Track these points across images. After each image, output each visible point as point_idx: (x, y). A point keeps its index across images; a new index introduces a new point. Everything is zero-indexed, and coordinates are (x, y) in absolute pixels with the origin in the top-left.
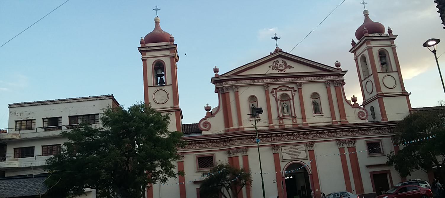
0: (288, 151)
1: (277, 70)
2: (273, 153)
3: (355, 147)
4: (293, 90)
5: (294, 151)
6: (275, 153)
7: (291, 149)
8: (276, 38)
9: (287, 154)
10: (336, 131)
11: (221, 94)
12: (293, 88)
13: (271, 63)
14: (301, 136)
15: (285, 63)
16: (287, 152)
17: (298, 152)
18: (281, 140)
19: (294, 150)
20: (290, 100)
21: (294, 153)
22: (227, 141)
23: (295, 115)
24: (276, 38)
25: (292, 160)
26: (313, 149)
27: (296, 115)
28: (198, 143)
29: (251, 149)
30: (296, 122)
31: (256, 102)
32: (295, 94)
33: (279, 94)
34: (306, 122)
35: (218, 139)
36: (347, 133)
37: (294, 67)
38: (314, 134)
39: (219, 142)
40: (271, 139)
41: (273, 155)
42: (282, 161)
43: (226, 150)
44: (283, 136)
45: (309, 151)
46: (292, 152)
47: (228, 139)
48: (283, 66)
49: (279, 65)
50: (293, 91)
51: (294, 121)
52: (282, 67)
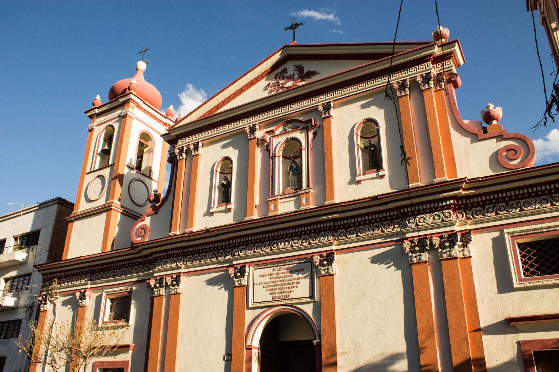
0: (267, 279)
3: (470, 257)
5: (284, 281)
7: (275, 274)
10: (402, 211)
15: (300, 69)
17: (291, 282)
23: (308, 186)
25: (276, 304)
28: (112, 270)
33: (278, 143)
36: (439, 216)
38: (341, 229)
42: (252, 306)
46: (277, 281)
48: (296, 76)
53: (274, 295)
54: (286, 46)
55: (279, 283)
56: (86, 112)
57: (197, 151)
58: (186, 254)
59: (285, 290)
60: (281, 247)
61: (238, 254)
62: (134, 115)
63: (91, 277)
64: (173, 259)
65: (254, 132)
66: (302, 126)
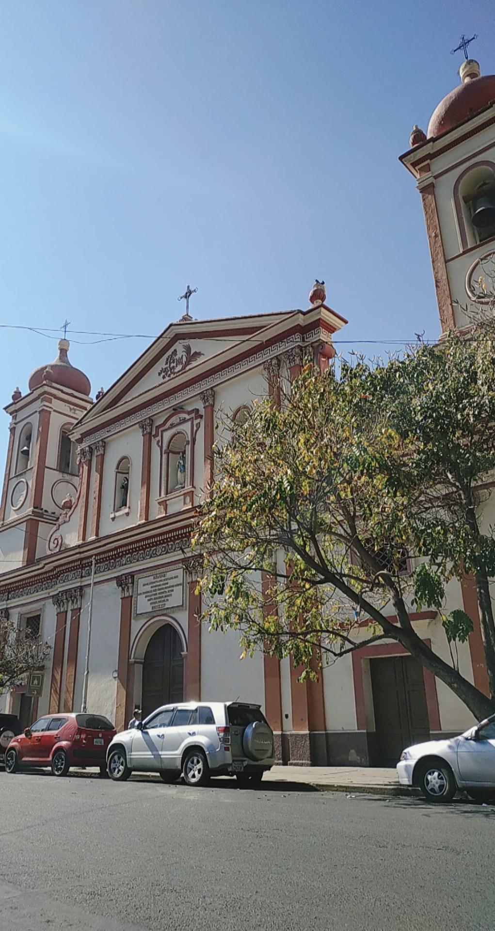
1: (172, 376)
4: (193, 415)
9: (146, 597)
13: (162, 364)
14: (177, 542)
15: (188, 349)
17: (166, 590)
18: (138, 561)
19: (160, 585)
21: (159, 594)
28: (25, 587)
29: (89, 591)
32: (198, 425)
33: (167, 435)
37: (204, 353)
39: (49, 578)
43: (53, 596)
44: (144, 549)
46: (155, 590)
48: (184, 359)
53: (154, 605)
54: (171, 325)
56: (5, 409)
59: (163, 599)
60: (158, 554)
62: (50, 408)
63: (8, 596)
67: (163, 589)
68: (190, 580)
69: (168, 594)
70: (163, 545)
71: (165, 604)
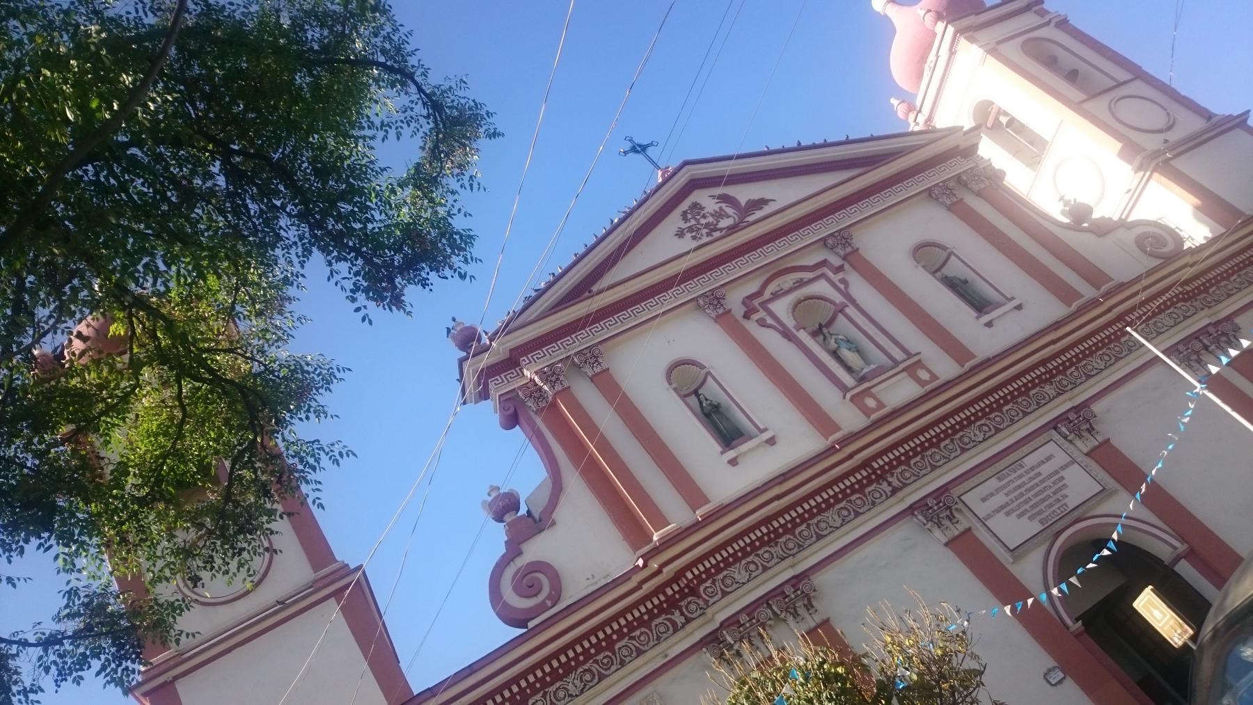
0: (1000, 499)
1: (717, 234)
2: (947, 545)
6: (955, 538)
7: (1008, 484)
8: (639, 149)
9: (1008, 514)
11: (536, 414)
12: (824, 263)
13: (674, 221)
16: (1002, 507)
17: (1049, 483)
19: (1024, 484)
20: (841, 311)
21: (1036, 495)
22: (682, 599)
24: (639, 149)
26: (1100, 439)
27: (913, 353)
28: (535, 692)
30: (934, 377)
31: (710, 379)
33: (781, 307)
34: (974, 357)
35: (629, 609)
39: (641, 622)
40: (885, 484)
41: (949, 553)
44: (932, 445)
45: (1087, 454)
46: (1022, 495)
47: (683, 582)
48: (730, 211)
49: (712, 215)
50: (831, 274)
51: (924, 375)
52: (728, 217)
54: (686, 163)
55: (1030, 494)
57: (599, 364)
58: (772, 536)
59: (1051, 500)
60: (981, 439)
61: (900, 484)
64: (744, 562)
65: (719, 302)
66: (810, 275)
67: (1037, 485)
68: (1085, 445)
69: (1056, 487)
70: (979, 423)
71: (1065, 504)
